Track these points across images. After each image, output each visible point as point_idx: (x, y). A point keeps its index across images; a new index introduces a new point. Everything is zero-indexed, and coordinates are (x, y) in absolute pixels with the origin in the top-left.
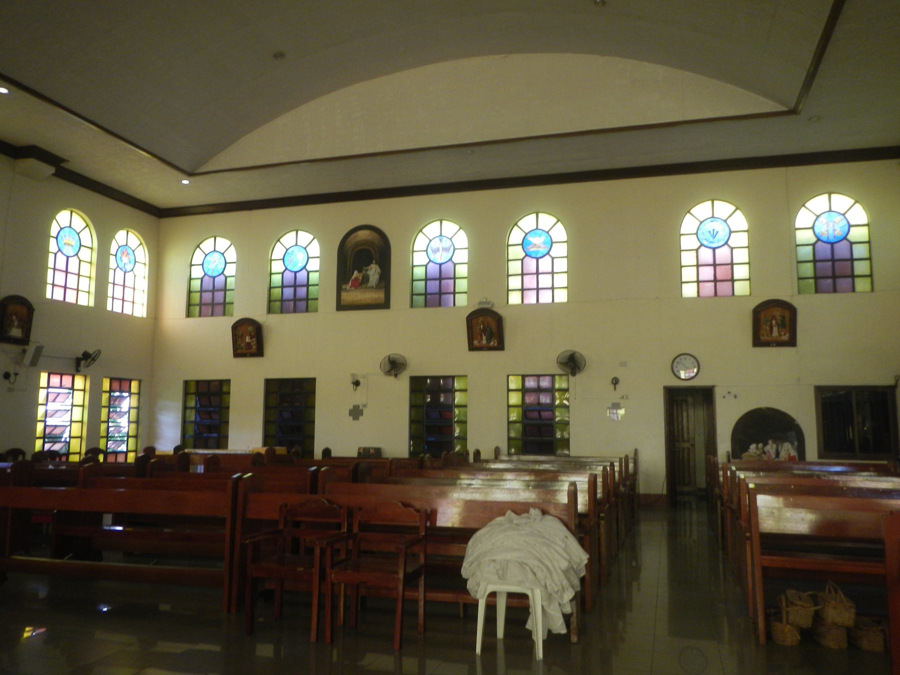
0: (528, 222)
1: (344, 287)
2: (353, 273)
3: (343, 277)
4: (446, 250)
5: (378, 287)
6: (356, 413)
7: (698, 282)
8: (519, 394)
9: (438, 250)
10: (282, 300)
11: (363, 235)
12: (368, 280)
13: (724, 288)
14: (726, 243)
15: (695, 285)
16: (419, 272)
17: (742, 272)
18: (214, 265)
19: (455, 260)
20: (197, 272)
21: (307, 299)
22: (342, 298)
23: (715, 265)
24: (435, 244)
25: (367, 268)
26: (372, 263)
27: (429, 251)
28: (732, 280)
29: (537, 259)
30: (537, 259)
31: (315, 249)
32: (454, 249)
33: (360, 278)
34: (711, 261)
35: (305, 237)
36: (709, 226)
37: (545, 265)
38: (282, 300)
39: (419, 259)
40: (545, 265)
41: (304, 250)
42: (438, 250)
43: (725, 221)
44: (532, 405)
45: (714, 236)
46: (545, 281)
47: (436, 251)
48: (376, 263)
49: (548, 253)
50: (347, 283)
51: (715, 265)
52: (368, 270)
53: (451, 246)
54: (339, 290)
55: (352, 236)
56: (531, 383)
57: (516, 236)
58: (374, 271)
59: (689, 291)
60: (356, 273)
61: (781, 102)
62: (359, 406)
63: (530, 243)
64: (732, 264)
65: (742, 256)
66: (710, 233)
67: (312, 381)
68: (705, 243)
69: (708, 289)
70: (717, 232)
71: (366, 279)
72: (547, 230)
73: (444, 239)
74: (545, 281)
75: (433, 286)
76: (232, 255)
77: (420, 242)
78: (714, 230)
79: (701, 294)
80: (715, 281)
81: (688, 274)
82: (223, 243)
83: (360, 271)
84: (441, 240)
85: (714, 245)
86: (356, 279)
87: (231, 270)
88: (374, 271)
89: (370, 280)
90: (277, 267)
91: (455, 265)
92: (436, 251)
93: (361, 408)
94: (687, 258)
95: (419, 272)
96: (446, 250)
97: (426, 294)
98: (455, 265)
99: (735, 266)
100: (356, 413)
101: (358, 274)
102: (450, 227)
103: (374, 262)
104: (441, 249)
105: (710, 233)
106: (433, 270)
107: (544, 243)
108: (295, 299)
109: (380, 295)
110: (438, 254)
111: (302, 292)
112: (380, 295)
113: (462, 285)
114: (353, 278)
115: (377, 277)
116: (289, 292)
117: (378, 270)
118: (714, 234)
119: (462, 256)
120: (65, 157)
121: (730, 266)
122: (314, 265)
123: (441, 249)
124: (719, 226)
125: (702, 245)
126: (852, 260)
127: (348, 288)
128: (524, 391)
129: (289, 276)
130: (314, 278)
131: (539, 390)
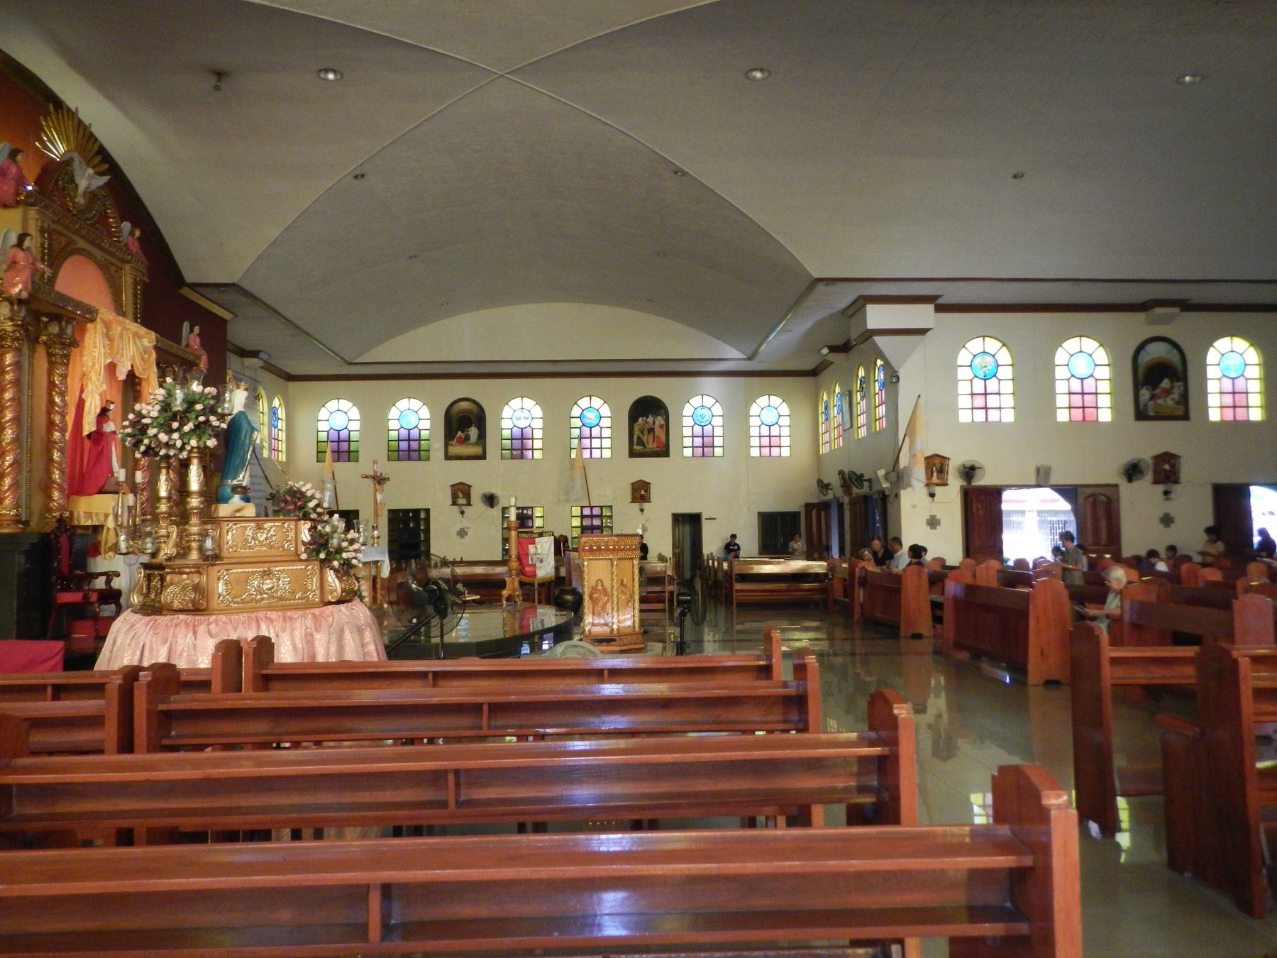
0: (584, 402)
3: (449, 436)
5: (477, 444)
6: (462, 533)
7: (693, 447)
8: (579, 519)
9: (520, 418)
10: (398, 451)
11: (464, 405)
16: (506, 433)
17: (718, 442)
18: (339, 422)
20: (323, 426)
21: (419, 450)
23: (703, 437)
24: (518, 414)
28: (713, 447)
29: (591, 428)
30: (591, 428)
31: (425, 412)
35: (415, 404)
36: (700, 412)
37: (596, 431)
38: (398, 451)
39: (506, 424)
40: (596, 431)
42: (520, 418)
44: (587, 526)
46: (596, 443)
47: (518, 419)
50: (452, 439)
51: (703, 437)
54: (446, 445)
55: (457, 405)
56: (587, 512)
57: (576, 411)
58: (473, 432)
60: (459, 433)
61: (744, 353)
64: (713, 436)
65: (719, 431)
71: (467, 438)
74: (596, 443)
75: (517, 443)
76: (355, 413)
77: (507, 412)
80: (703, 447)
81: (688, 442)
82: (345, 404)
83: (463, 432)
85: (703, 424)
86: (460, 437)
87: (355, 426)
88: (473, 432)
90: (393, 425)
91: (533, 429)
92: (518, 419)
94: (687, 432)
95: (506, 433)
97: (512, 449)
98: (533, 429)
100: (462, 533)
102: (529, 403)
106: (517, 432)
108: (409, 450)
109: (478, 450)
111: (414, 445)
112: (478, 450)
113: (538, 444)
115: (476, 436)
116: (404, 445)
117: (477, 431)
118: (702, 416)
119: (538, 423)
120: (258, 349)
122: (425, 425)
124: (705, 412)
128: (583, 517)
129: (404, 433)
130: (425, 434)
131: (592, 517)
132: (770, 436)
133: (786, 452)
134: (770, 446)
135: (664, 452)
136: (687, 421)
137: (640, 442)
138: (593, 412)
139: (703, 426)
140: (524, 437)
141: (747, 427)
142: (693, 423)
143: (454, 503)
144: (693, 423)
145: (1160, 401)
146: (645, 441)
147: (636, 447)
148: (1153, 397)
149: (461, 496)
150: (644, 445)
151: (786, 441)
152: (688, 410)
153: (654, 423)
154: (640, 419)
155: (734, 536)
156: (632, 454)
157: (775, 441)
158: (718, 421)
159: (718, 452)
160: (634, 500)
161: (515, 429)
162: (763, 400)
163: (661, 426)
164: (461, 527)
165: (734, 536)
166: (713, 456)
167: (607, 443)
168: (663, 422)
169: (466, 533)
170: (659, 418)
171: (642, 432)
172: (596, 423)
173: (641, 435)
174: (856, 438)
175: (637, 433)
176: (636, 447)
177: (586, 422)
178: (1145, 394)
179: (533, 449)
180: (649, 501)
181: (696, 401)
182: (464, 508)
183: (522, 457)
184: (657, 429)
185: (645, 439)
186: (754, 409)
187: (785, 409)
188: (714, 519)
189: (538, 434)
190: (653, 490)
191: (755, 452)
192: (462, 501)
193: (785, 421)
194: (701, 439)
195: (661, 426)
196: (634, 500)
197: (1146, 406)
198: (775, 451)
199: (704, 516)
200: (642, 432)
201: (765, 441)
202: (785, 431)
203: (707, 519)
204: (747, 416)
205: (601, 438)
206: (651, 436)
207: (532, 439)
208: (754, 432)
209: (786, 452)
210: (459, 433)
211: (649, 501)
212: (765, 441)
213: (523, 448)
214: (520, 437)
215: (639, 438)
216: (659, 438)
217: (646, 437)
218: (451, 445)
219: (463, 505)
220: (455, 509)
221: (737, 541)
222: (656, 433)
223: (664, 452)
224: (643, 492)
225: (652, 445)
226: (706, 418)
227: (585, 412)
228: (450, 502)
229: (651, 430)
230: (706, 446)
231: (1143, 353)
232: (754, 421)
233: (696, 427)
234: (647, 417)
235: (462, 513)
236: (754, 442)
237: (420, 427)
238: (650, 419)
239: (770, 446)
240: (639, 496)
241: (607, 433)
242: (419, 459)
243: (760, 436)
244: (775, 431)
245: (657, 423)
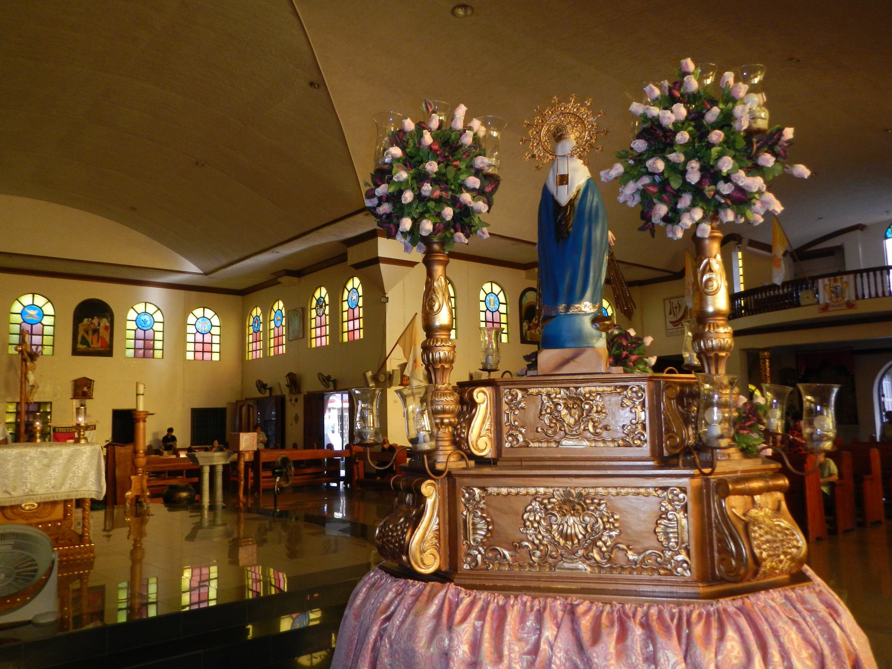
7: (135, 349)
8: (14, 415)
17: (158, 345)
28: (153, 349)
30: (32, 325)
34: (142, 337)
51: (144, 340)
57: (17, 307)
61: (201, 270)
63: (27, 313)
65: (159, 336)
68: (140, 327)
80: (145, 349)
85: (145, 329)
94: (130, 334)
107: (37, 315)
118: (145, 321)
124: (147, 317)
125: (138, 328)
126: (212, 343)
132: (203, 343)
133: (216, 357)
134: (203, 352)
135: (107, 351)
136: (131, 325)
137: (85, 341)
138: (34, 310)
139: (145, 331)
141: (184, 333)
145: (533, 331)
148: (529, 329)
150: (88, 345)
151: (216, 348)
152: (132, 315)
153: (99, 324)
154: (86, 320)
155: (170, 430)
156: (76, 352)
157: (207, 347)
158: (158, 327)
159: (158, 354)
160: (75, 396)
162: (199, 312)
165: (170, 430)
166: (153, 358)
168: (108, 324)
170: (105, 320)
171: (87, 332)
172: (39, 320)
173: (86, 335)
174: (309, 346)
175: (81, 332)
176: (80, 346)
177: (28, 318)
178: (526, 325)
180: (91, 398)
181: (140, 308)
184: (102, 331)
185: (89, 338)
186: (191, 319)
187: (216, 321)
188: (152, 414)
190: (96, 387)
191: (190, 356)
193: (216, 331)
195: (106, 328)
196: (75, 396)
197: (526, 333)
198: (207, 356)
200: (87, 332)
201: (199, 347)
202: (216, 339)
204: (185, 324)
206: (96, 336)
208: (190, 338)
209: (216, 357)
211: (91, 398)
212: (199, 347)
215: (83, 338)
216: (103, 339)
217: (90, 336)
221: (174, 434)
222: (101, 334)
223: (107, 351)
224: (85, 389)
225: (96, 345)
226: (149, 323)
227: (26, 309)
229: (96, 331)
230: (146, 349)
231: (524, 298)
232: (191, 329)
234: (93, 318)
236: (190, 347)
238: (96, 321)
239: (203, 352)
240: (80, 392)
243: (195, 343)
244: (207, 338)
245: (102, 324)
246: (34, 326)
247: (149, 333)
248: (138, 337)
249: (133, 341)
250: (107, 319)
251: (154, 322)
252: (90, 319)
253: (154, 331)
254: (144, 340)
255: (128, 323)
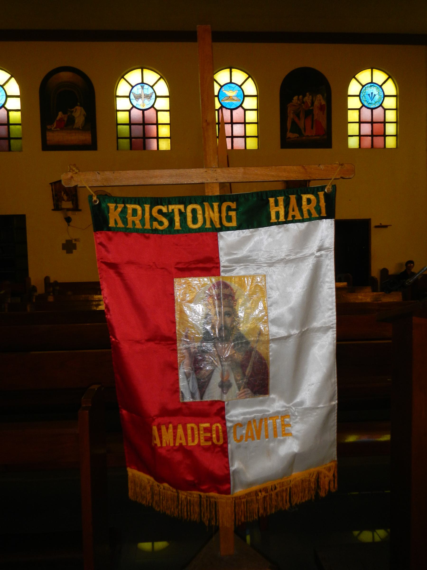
1: (48, 127)
2: (57, 115)
4: (148, 97)
5: (84, 129)
7: (360, 136)
11: (65, 76)
12: (74, 121)
13: (378, 141)
14: (381, 105)
15: (357, 138)
17: (391, 129)
19: (157, 106)
22: (48, 138)
24: (137, 90)
25: (72, 110)
26: (77, 105)
27: (132, 97)
28: (385, 136)
30: (232, 110)
32: (156, 97)
33: (66, 119)
34: (369, 119)
41: (2, 89)
43: (381, 86)
45: (372, 99)
46: (238, 130)
47: (138, 97)
48: (81, 106)
49: (241, 106)
51: (372, 122)
52: (73, 111)
53: (152, 93)
59: (353, 143)
60: (60, 113)
62: (71, 241)
64: (384, 122)
65: (391, 116)
66: (369, 96)
67: (22, 218)
68: (366, 104)
69: (367, 142)
70: (375, 95)
71: (71, 121)
72: (240, 84)
73: (146, 86)
75: (138, 131)
78: (372, 93)
79: (362, 146)
80: (372, 135)
81: (353, 129)
83: (64, 113)
84: (143, 88)
85: (372, 106)
86: (61, 120)
89: (76, 122)
91: (157, 111)
92: (138, 97)
93: (74, 242)
94: (353, 116)
96: (148, 97)
97: (130, 138)
99: (387, 125)
101: (63, 116)
103: (79, 104)
104: (143, 96)
105: (369, 96)
109: (86, 137)
110: (140, 101)
112: (86, 137)
113: (165, 131)
114: (58, 118)
117: (83, 112)
118: (372, 96)
121: (383, 124)
123: (143, 96)
124: (374, 90)
125: (363, 105)
127: (53, 128)
137: (296, 128)
139: (372, 109)
140: (146, 122)
142: (359, 105)
143: (57, 208)
144: (359, 105)
146: (302, 126)
147: (290, 135)
149: (65, 197)
150: (300, 133)
153: (313, 103)
154: (295, 98)
158: (390, 103)
161: (134, 111)
163: (321, 108)
164: (68, 238)
167: (252, 130)
168: (323, 102)
169: (74, 247)
170: (319, 96)
171: (298, 115)
175: (291, 116)
176: (290, 135)
179: (158, 138)
182: (70, 214)
183: (144, 147)
184: (316, 112)
185: (301, 124)
188: (386, 226)
189: (164, 117)
192: (67, 205)
194: (369, 125)
195: (321, 108)
199: (373, 224)
200: (298, 115)
203: (376, 227)
205: (245, 123)
207: (157, 124)
210: (60, 113)
213: (145, 137)
214: (141, 122)
215: (293, 123)
218: (50, 130)
219: (68, 210)
220: (59, 216)
226: (377, 97)
227: (223, 89)
228: (50, 204)
229: (309, 113)
233: (364, 109)
234: (304, 96)
235: (68, 220)
237: (8, 106)
238: (308, 99)
241: (252, 116)
242: (10, 150)
245: (316, 103)
246: (234, 112)
247: (378, 113)
248: (363, 119)
249: (357, 125)
250: (323, 96)
251: (385, 96)
252: (301, 97)
253: (385, 110)
254: (372, 122)
255: (350, 99)
